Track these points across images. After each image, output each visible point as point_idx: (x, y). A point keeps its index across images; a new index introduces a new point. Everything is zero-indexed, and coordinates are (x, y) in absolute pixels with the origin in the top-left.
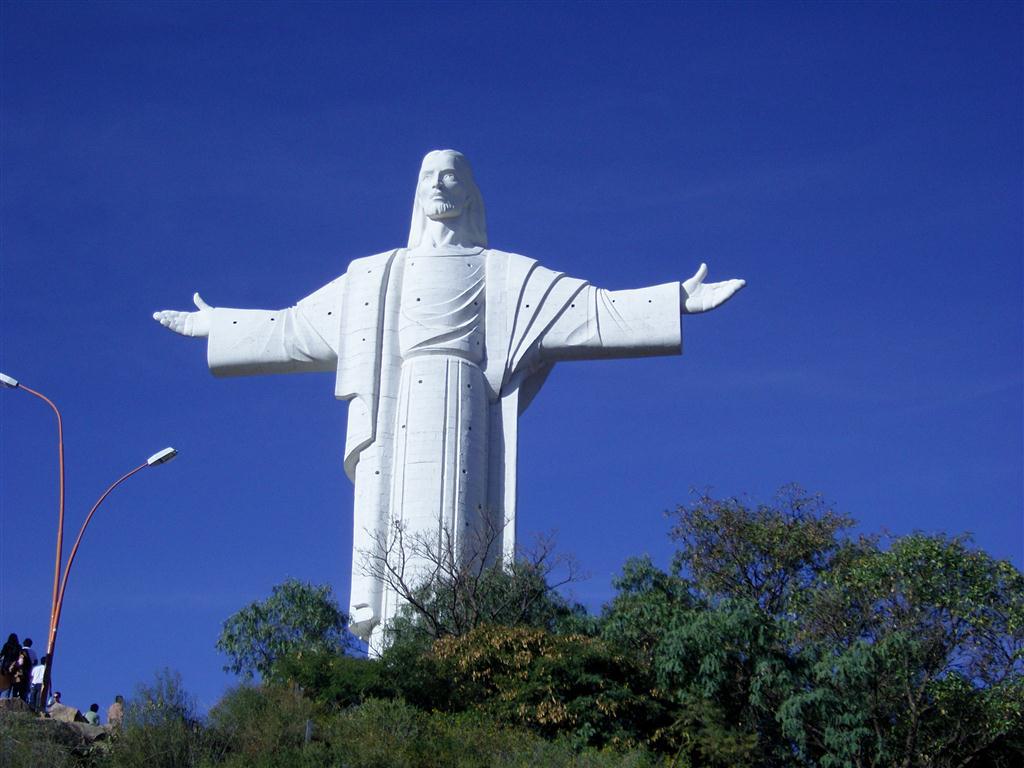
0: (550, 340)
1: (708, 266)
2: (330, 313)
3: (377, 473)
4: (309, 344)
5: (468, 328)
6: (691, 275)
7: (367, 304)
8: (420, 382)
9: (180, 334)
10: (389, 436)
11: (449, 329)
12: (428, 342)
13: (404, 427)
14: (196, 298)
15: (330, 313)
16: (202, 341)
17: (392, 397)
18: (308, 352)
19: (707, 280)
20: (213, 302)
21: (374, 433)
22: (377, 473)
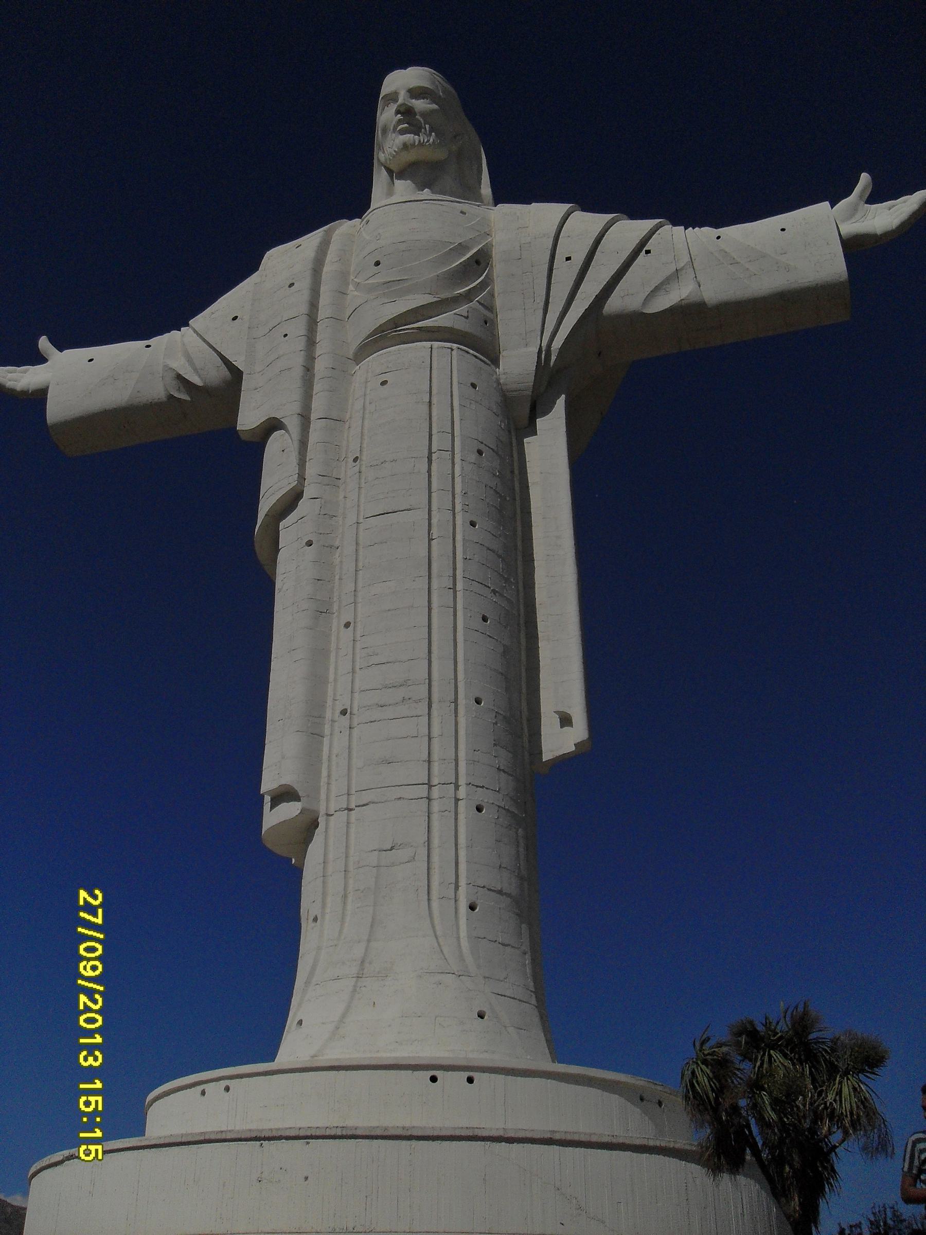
0: (614, 304)
1: (874, 179)
2: (235, 318)
3: (309, 544)
4: (196, 370)
5: (468, 297)
6: (848, 193)
7: (291, 285)
8: (384, 383)
9: (12, 390)
10: (332, 481)
11: (430, 299)
12: (396, 322)
13: (355, 460)
14: (44, 343)
15: (235, 318)
16: (39, 397)
17: (336, 421)
18: (196, 380)
19: (875, 197)
20: (61, 346)
21: (302, 478)
22: (309, 544)
